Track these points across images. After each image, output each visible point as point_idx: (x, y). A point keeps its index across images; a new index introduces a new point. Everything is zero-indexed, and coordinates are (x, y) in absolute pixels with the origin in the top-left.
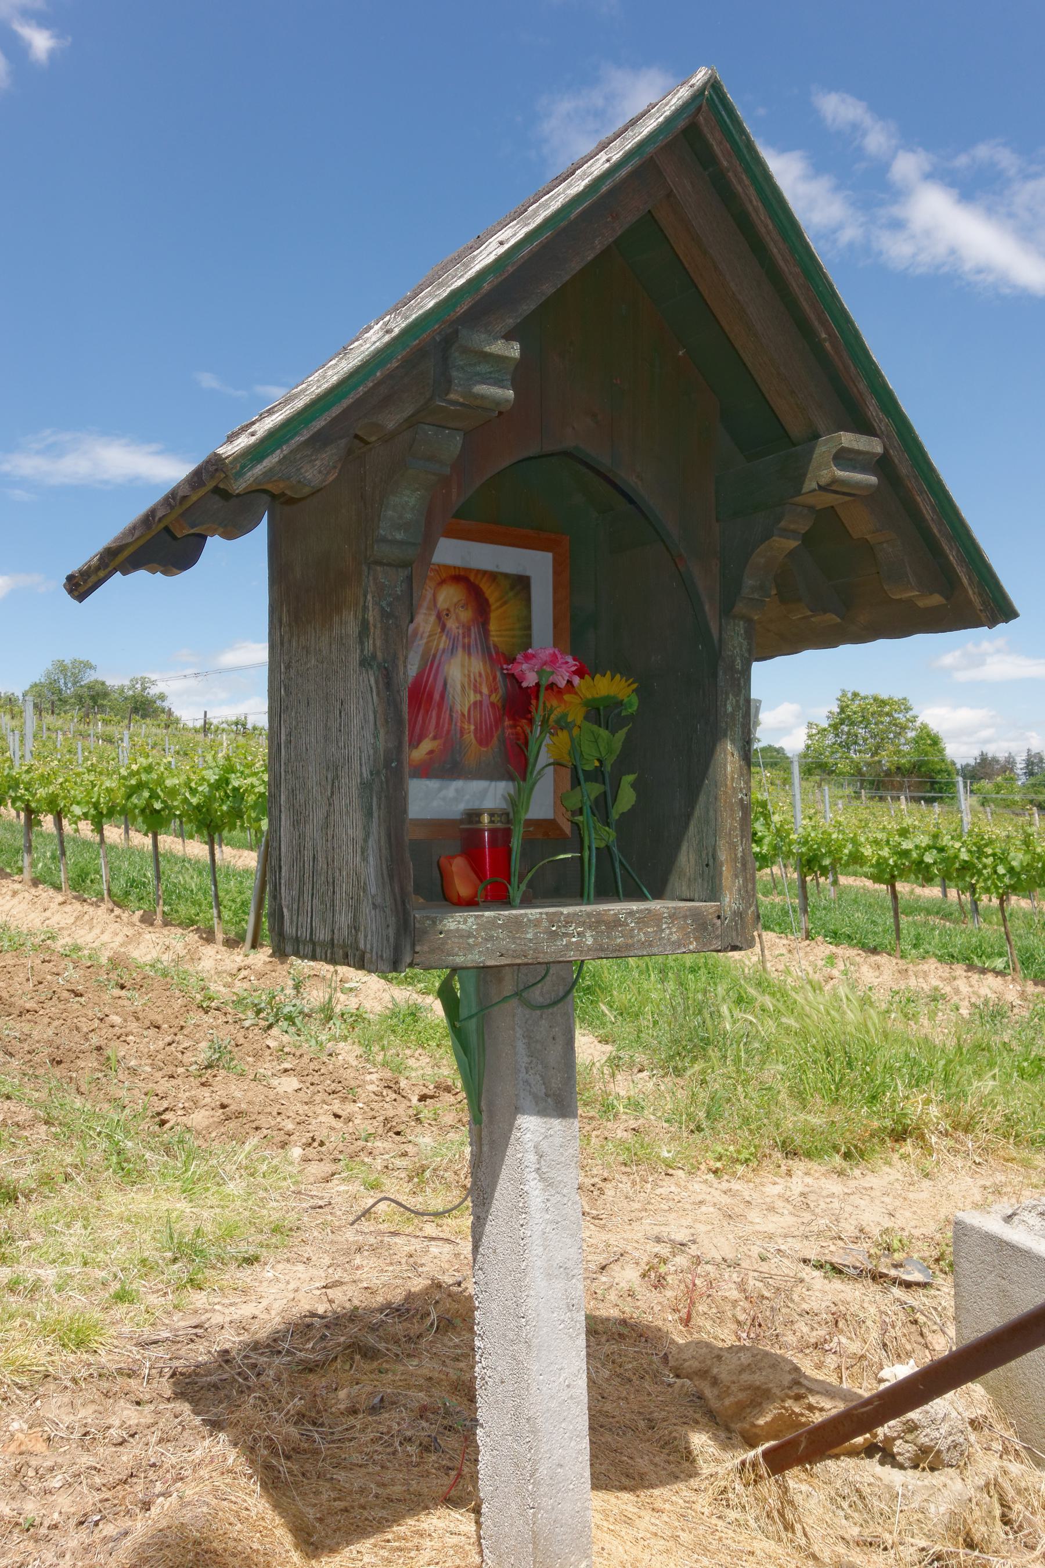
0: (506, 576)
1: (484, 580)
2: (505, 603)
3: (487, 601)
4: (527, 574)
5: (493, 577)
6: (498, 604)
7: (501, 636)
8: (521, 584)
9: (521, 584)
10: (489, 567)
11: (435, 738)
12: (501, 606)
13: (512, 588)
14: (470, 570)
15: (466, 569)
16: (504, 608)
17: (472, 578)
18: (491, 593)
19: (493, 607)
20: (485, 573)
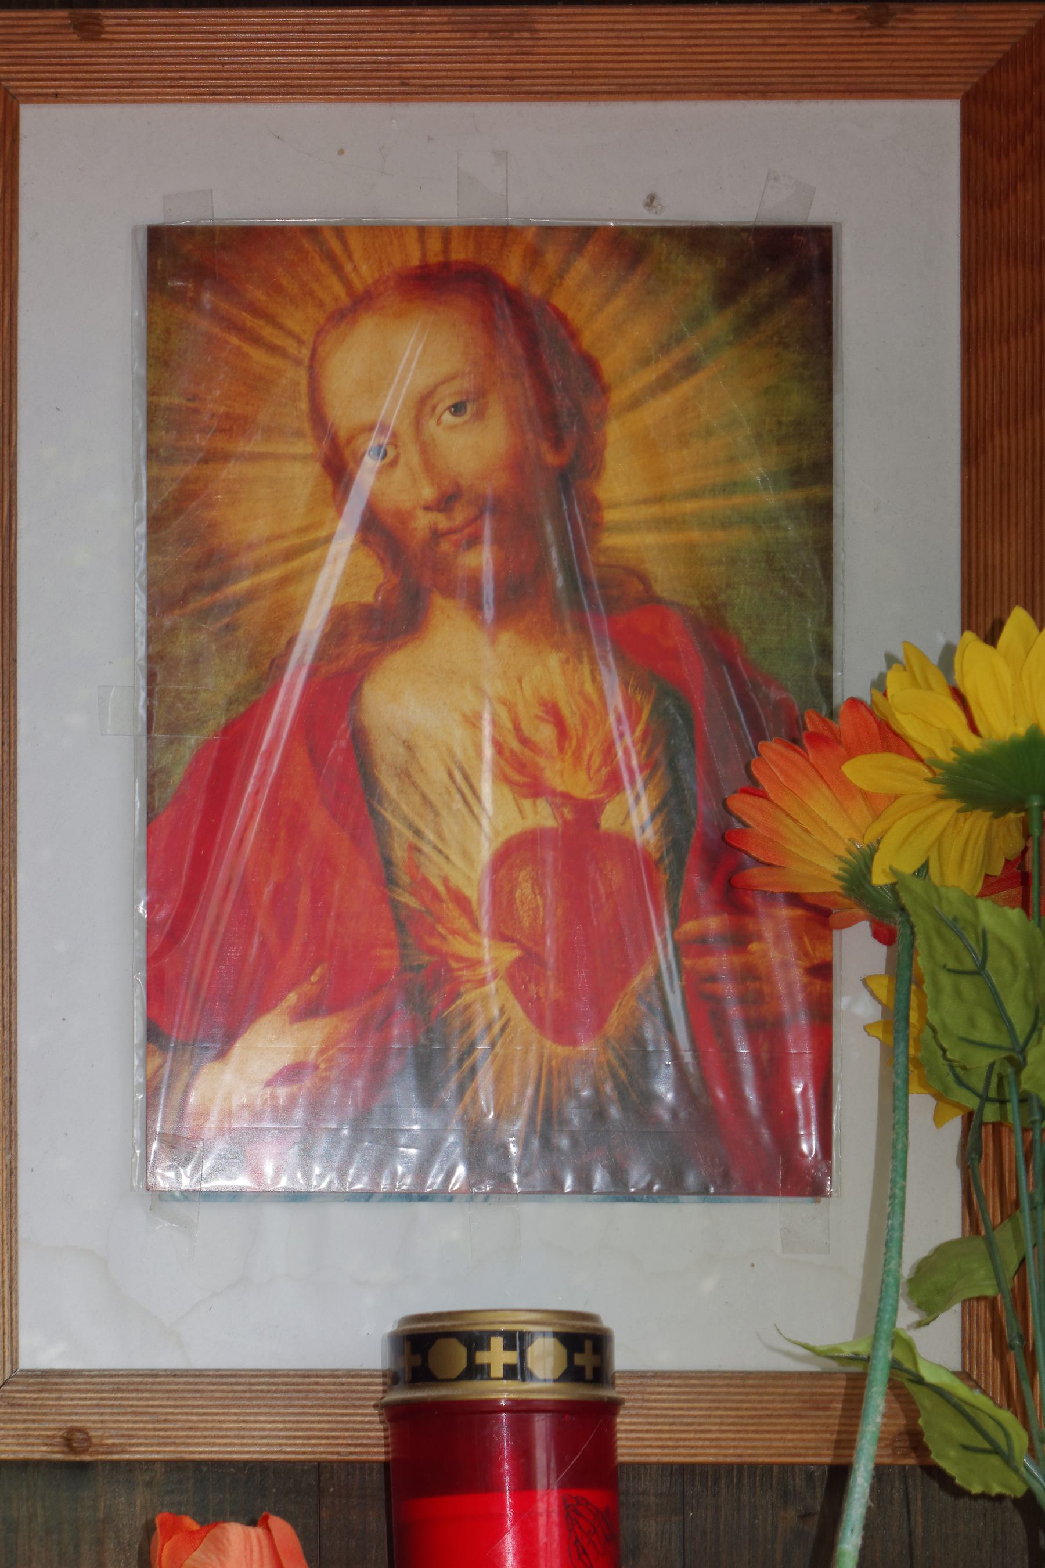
0: (699, 239)
1: (582, 266)
2: (690, 366)
3: (591, 365)
4: (815, 216)
5: (631, 249)
6: (650, 375)
7: (666, 523)
8: (778, 278)
9: (778, 278)
10: (619, 206)
11: (307, 1012)
12: (665, 384)
13: (727, 292)
14: (505, 234)
15: (477, 233)
16: (686, 388)
17: (512, 269)
18: (616, 327)
19: (619, 396)
20: (582, 236)
